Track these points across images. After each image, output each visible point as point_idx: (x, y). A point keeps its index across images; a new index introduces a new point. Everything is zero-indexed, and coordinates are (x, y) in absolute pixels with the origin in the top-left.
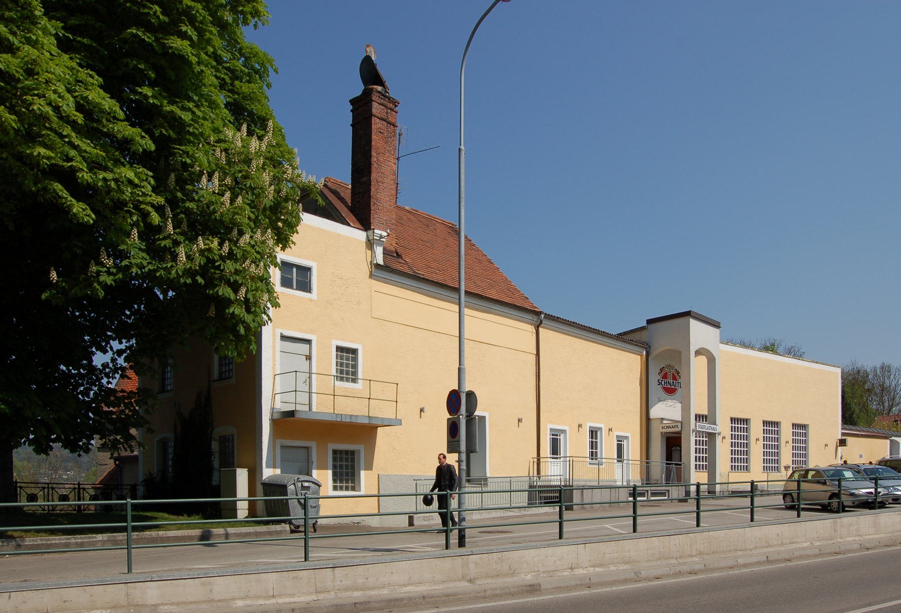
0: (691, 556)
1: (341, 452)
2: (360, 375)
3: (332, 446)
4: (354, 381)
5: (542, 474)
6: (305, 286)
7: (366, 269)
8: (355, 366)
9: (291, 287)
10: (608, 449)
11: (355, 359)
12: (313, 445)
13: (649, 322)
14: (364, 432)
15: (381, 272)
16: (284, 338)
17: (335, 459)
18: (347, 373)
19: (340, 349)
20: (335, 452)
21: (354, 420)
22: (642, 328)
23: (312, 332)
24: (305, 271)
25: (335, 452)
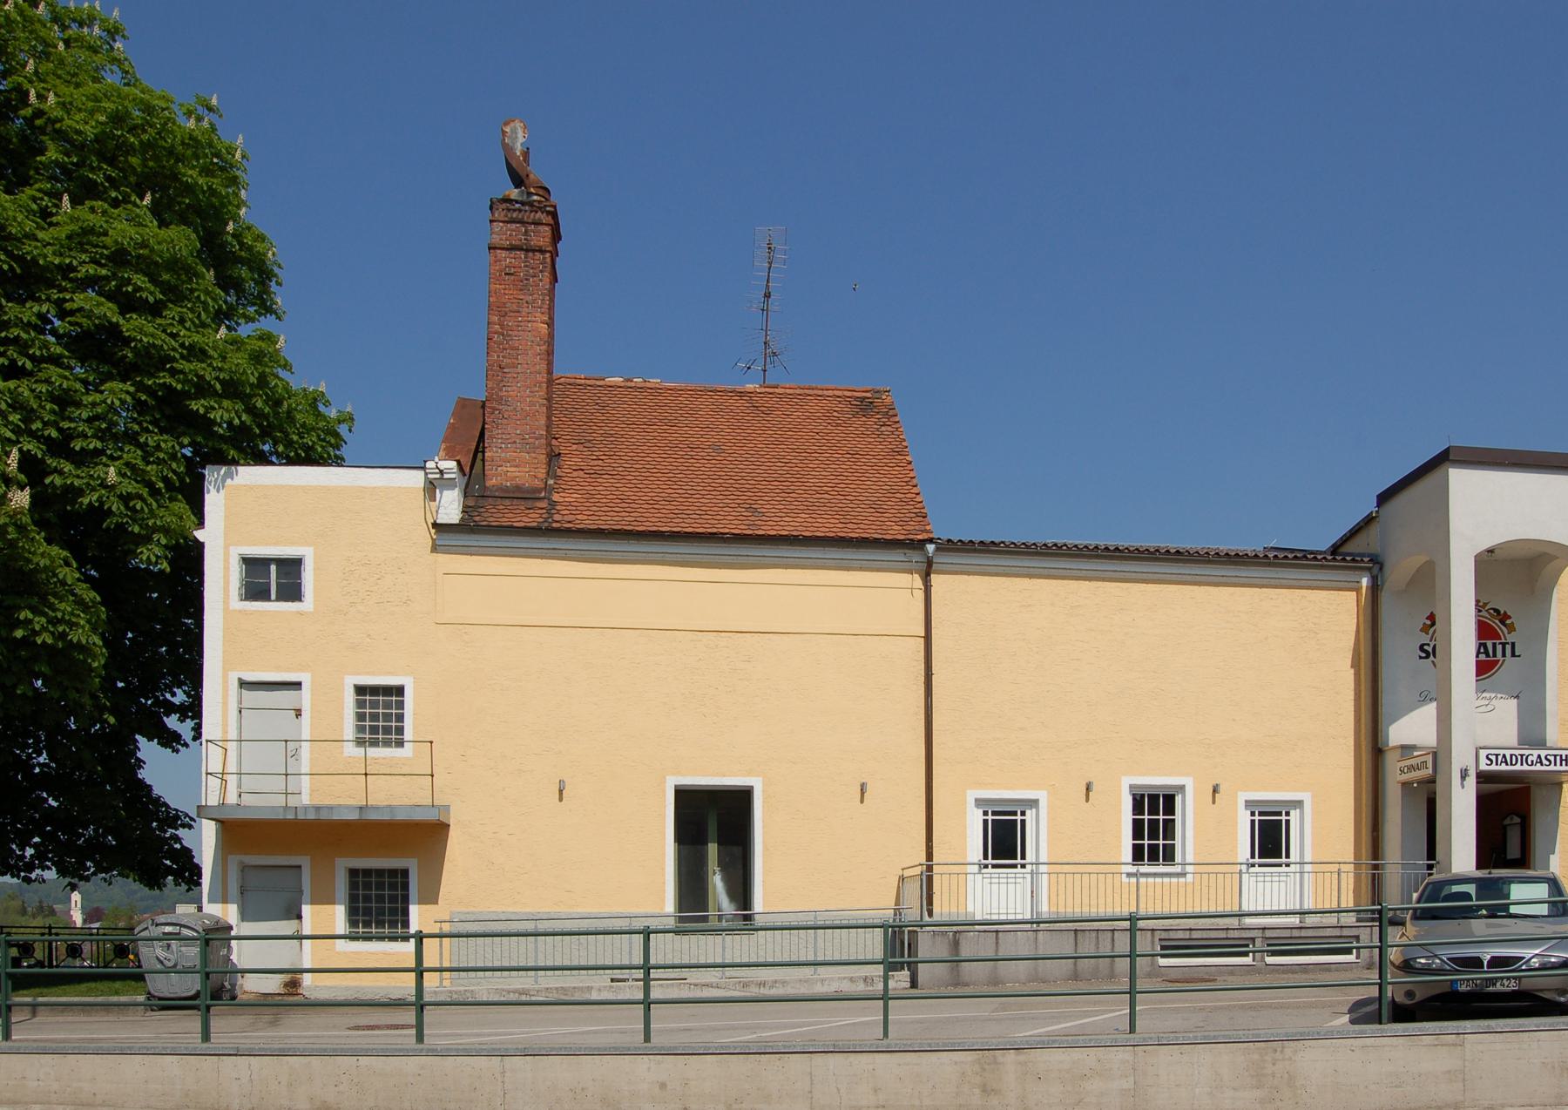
2: (408, 734)
3: (342, 865)
4: (400, 744)
6: (292, 592)
7: (425, 537)
8: (400, 718)
10: (1212, 833)
11: (401, 705)
12: (305, 862)
13: (1383, 498)
14: (426, 835)
16: (243, 684)
17: (353, 886)
18: (387, 730)
19: (360, 690)
20: (353, 873)
22: (1369, 520)
23: (302, 668)
24: (291, 567)
25: (353, 873)
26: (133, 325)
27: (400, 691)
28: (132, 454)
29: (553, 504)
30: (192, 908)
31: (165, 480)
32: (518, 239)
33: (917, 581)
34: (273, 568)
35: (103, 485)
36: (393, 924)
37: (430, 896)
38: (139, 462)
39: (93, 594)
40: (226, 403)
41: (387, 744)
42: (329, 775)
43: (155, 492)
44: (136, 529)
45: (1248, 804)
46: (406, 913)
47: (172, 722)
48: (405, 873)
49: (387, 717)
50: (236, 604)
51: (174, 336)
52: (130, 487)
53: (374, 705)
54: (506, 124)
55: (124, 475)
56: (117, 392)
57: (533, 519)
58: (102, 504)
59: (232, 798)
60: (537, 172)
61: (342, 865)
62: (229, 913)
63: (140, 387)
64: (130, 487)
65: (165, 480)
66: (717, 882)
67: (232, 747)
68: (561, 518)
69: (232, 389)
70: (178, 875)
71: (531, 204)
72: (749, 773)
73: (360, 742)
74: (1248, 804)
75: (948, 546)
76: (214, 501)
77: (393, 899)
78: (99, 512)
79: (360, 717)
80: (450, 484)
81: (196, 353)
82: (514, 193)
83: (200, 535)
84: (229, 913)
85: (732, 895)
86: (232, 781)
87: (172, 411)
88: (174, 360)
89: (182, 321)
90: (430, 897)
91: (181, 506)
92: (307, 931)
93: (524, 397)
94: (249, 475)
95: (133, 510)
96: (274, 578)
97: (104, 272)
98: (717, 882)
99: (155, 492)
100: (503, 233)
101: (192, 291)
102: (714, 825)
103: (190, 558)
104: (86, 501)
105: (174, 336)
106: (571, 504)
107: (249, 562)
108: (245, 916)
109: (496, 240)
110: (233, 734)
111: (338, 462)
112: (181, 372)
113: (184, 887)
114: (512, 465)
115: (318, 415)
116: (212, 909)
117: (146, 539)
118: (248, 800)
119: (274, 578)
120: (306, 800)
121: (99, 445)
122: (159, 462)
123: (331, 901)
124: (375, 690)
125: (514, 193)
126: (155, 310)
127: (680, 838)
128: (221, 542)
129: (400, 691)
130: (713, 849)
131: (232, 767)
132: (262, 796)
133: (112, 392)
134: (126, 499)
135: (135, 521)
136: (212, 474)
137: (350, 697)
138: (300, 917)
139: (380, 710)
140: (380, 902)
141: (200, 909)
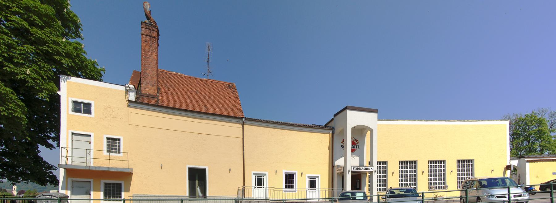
1: (110, 184)
2: (121, 151)
3: (103, 182)
4: (119, 153)
7: (126, 103)
8: (119, 146)
9: (81, 112)
10: (301, 183)
11: (119, 143)
12: (92, 180)
18: (116, 149)
19: (108, 139)
20: (106, 184)
25: (106, 184)
26: (33, 30)
27: (119, 140)
28: (34, 67)
29: (159, 100)
30: (56, 191)
31: (47, 76)
33: (241, 127)
34: (82, 105)
35: (25, 73)
36: (117, 197)
37: (127, 190)
38: (39, 71)
39: (22, 103)
40: (66, 59)
41: (116, 152)
42: (98, 158)
43: (43, 79)
44: (37, 88)
45: (308, 177)
46: (121, 194)
48: (121, 184)
49: (116, 146)
50: (71, 112)
51: (49, 37)
52: (35, 76)
53: (112, 143)
55: (33, 72)
56: (29, 48)
57: (154, 102)
58: (25, 79)
59: (69, 163)
60: (153, 17)
61: (103, 182)
62: (69, 193)
63: (37, 48)
64: (35, 76)
65: (47, 76)
66: (198, 189)
67: (70, 150)
68: (161, 103)
69: (68, 55)
70: (51, 182)
71: (152, 25)
72: (205, 165)
73: (108, 152)
74: (308, 177)
75: (247, 119)
76: (63, 84)
77: (117, 191)
78: (24, 81)
79: (108, 145)
80: (132, 91)
81: (58, 44)
82: (147, 21)
83: (59, 93)
84: (69, 193)
85: (202, 192)
86: (70, 159)
87: (49, 57)
88: (48, 43)
89: (51, 33)
90: (127, 190)
91: (52, 84)
92: (92, 198)
93: (151, 72)
94: (73, 79)
95: (36, 82)
96: (82, 108)
98: (198, 189)
99: (43, 79)
100: (144, 31)
101: (54, 25)
102: (197, 176)
104: (19, 77)
105: (49, 37)
106: (163, 100)
107: (75, 103)
108: (72, 194)
109: (143, 32)
110: (70, 146)
112: (51, 47)
113: (53, 186)
114: (148, 89)
116: (62, 192)
117: (41, 91)
118: (74, 164)
119: (82, 108)
120: (92, 165)
121: (23, 62)
122: (45, 71)
123: (100, 191)
124: (112, 139)
125: (147, 21)
126: (42, 28)
127: (190, 179)
128: (66, 96)
129: (119, 140)
130: (197, 182)
131: (70, 154)
132: (79, 162)
133: (27, 47)
134: (34, 79)
135: (37, 86)
136: (62, 78)
137: (105, 141)
138: (90, 194)
139: (114, 144)
141: (58, 192)
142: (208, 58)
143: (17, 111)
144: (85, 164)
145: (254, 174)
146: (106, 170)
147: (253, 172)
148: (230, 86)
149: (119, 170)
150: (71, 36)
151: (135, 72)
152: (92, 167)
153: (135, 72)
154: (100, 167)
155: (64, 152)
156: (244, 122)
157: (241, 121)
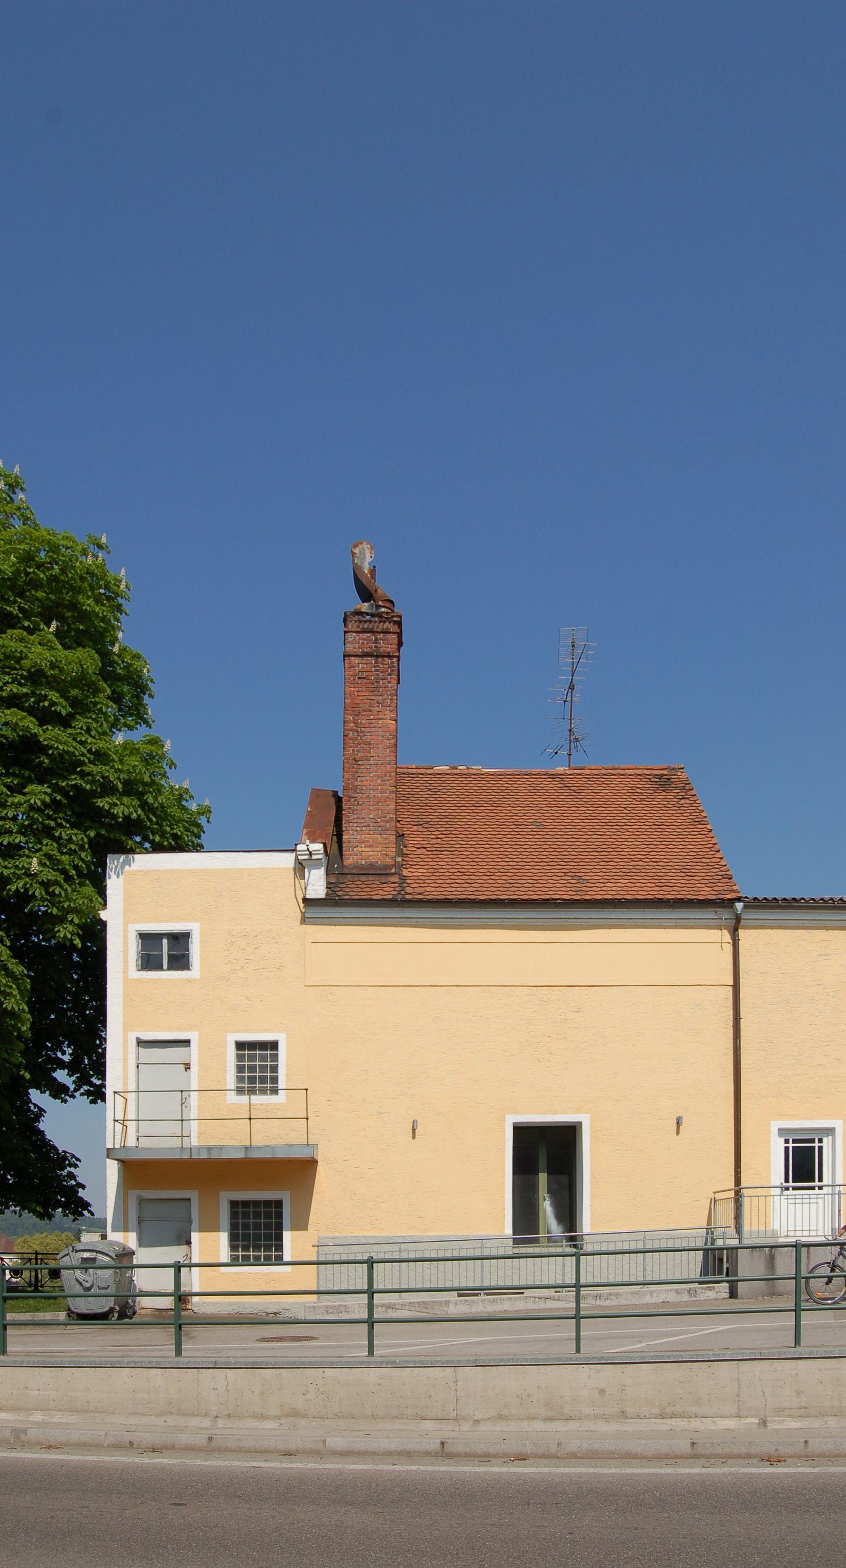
0: (263, 1417)
1: (246, 1204)
2: (282, 1084)
3: (226, 1197)
4: (275, 1091)
5: (746, 1227)
6: (180, 961)
7: (295, 910)
8: (275, 1069)
9: (159, 967)
11: (275, 1058)
12: (194, 1195)
14: (299, 1170)
15: (319, 909)
16: (141, 1043)
17: (234, 1215)
18: (263, 1080)
19: (240, 1046)
20: (234, 1204)
21: (215, 1155)
23: (191, 1028)
24: (180, 940)
25: (234, 1204)
26: (49, 735)
27: (274, 1045)
28: (49, 847)
29: (403, 879)
30: (96, 1237)
31: (76, 867)
32: (370, 647)
34: (165, 941)
35: (28, 874)
36: (268, 1248)
37: (301, 1224)
38: (56, 853)
39: (21, 968)
40: (126, 800)
41: (263, 1091)
42: (216, 1120)
43: (68, 879)
44: (55, 911)
46: (280, 1238)
47: (62, 1076)
48: (279, 1204)
49: (263, 1069)
50: (135, 973)
51: (82, 743)
52: (51, 875)
53: (252, 1058)
54: (355, 546)
55: (44, 865)
56: (38, 793)
57: (387, 892)
58: (27, 890)
59: (131, 1142)
60: (383, 587)
61: (226, 1197)
62: (131, 1240)
63: (56, 789)
64: (51, 875)
65: (76, 867)
66: (547, 1207)
67: (131, 1097)
68: (413, 891)
69: (130, 788)
71: (380, 615)
72: (578, 1110)
73: (240, 1091)
76: (114, 885)
77: (268, 1226)
78: (24, 897)
79: (240, 1069)
80: (316, 864)
81: (100, 757)
82: (365, 607)
83: (103, 915)
84: (131, 1240)
85: (560, 1218)
86: (132, 1126)
87: (81, 809)
88: (82, 764)
89: (88, 731)
90: (301, 1224)
91: (89, 890)
93: (375, 785)
94: (146, 863)
95: (52, 894)
96: (166, 951)
97: (25, 690)
98: (547, 1207)
99: (68, 879)
100: (356, 642)
101: (95, 704)
102: (547, 1157)
103: (95, 933)
104: (13, 888)
105: (82, 743)
106: (419, 878)
107: (143, 936)
108: (142, 1243)
109: (350, 648)
110: (132, 1086)
111: (198, 848)
112: (89, 774)
114: (367, 846)
115: (184, 808)
116: (114, 1236)
117: (62, 920)
118: (144, 1143)
119: (166, 951)
120: (195, 1142)
121: (23, 839)
122: (72, 852)
123: (217, 1229)
124: (252, 1045)
125: (365, 607)
126: (65, 722)
127: (516, 1171)
128: (121, 919)
129: (274, 1045)
130: (543, 1178)
131: (131, 1115)
132: (158, 1138)
133: (32, 793)
134: (46, 885)
135: (53, 905)
136: (113, 862)
137: (232, 1052)
138: (189, 1243)
139: (257, 1063)
140: (258, 1231)
141: (104, 1237)
142: (572, 687)
143: (10, 994)
144: (176, 1143)
145: (782, 1132)
146: (240, 1155)
147: (775, 1126)
148: (664, 781)
149: (280, 1155)
150: (125, 725)
151: (317, 794)
152: (199, 1149)
153: (317, 794)
154: (221, 1148)
155: (112, 1106)
156: (738, 919)
157: (725, 914)
